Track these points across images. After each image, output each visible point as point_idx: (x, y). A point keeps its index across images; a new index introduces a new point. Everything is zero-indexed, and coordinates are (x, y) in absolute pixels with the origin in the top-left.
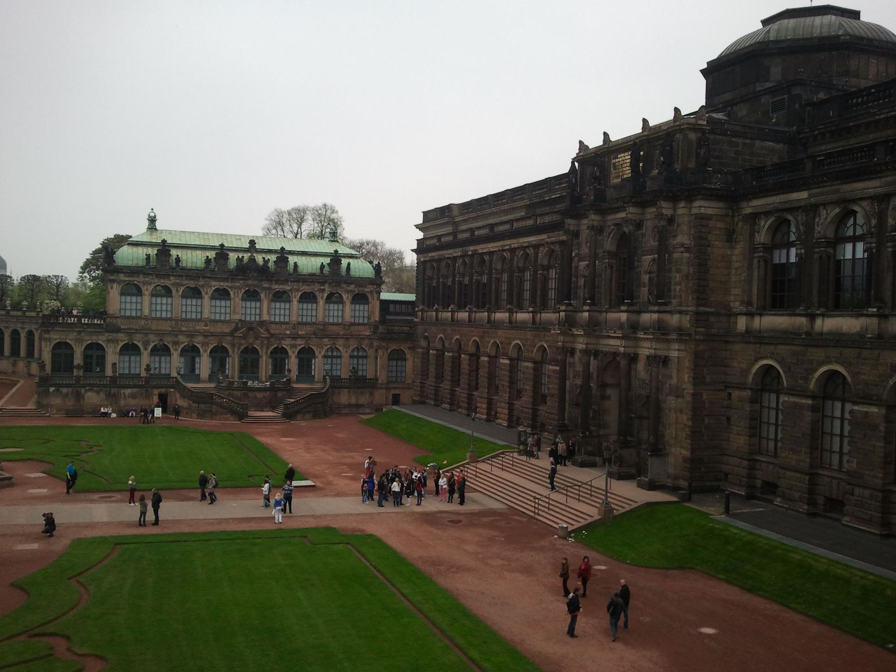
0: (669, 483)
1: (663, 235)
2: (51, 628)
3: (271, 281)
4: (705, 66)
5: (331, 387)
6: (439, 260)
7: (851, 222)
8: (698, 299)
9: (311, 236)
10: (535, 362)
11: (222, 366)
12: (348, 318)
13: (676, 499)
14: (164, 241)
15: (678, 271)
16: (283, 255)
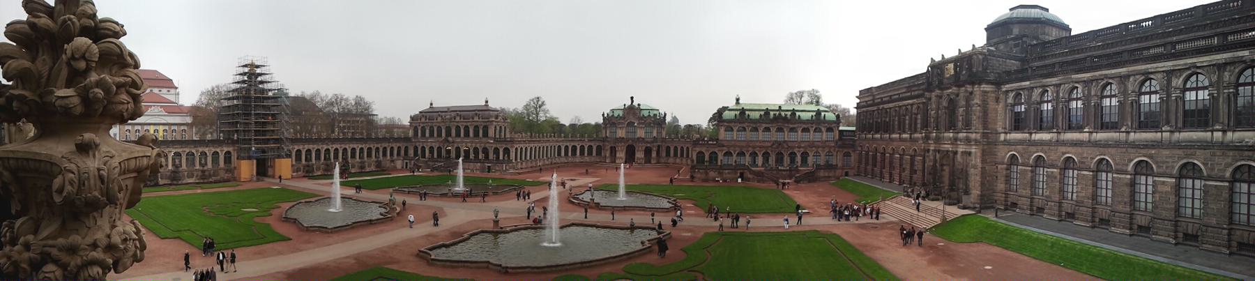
0: (972, 206)
1: (968, 100)
2: (696, 269)
3: (788, 123)
4: (986, 27)
5: (817, 169)
6: (867, 112)
7: (1046, 95)
8: (984, 127)
9: (807, 103)
10: (911, 156)
11: (768, 160)
12: (824, 138)
13: (974, 212)
14: (743, 108)
15: (975, 115)
16: (794, 112)
